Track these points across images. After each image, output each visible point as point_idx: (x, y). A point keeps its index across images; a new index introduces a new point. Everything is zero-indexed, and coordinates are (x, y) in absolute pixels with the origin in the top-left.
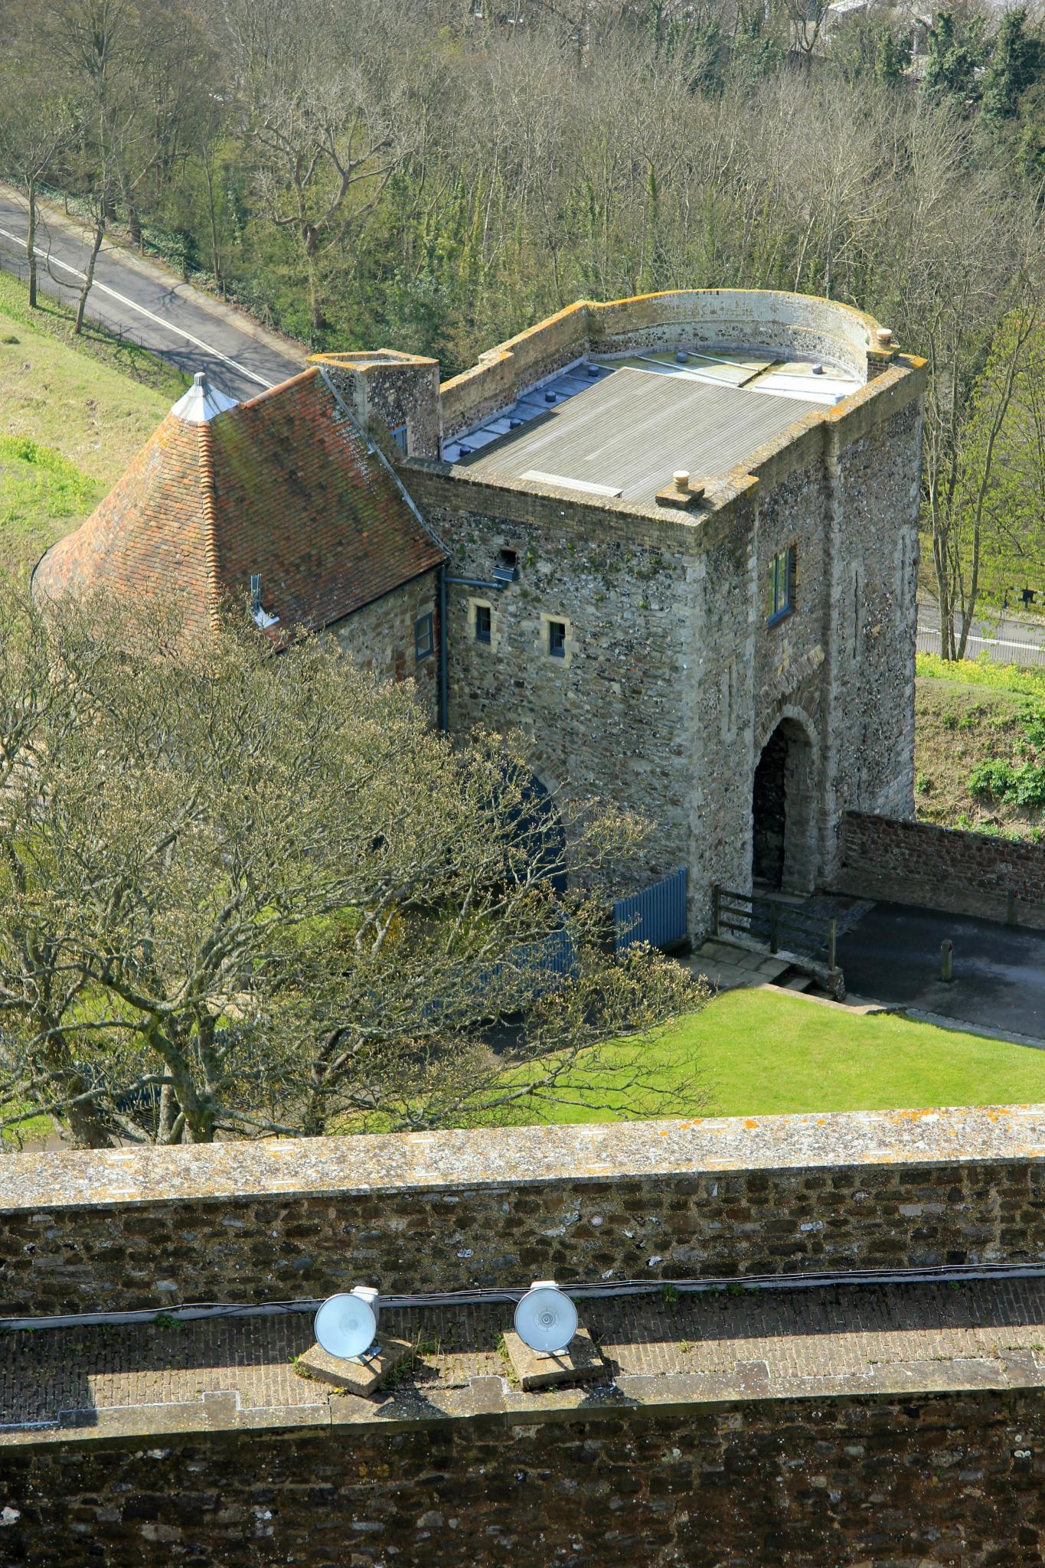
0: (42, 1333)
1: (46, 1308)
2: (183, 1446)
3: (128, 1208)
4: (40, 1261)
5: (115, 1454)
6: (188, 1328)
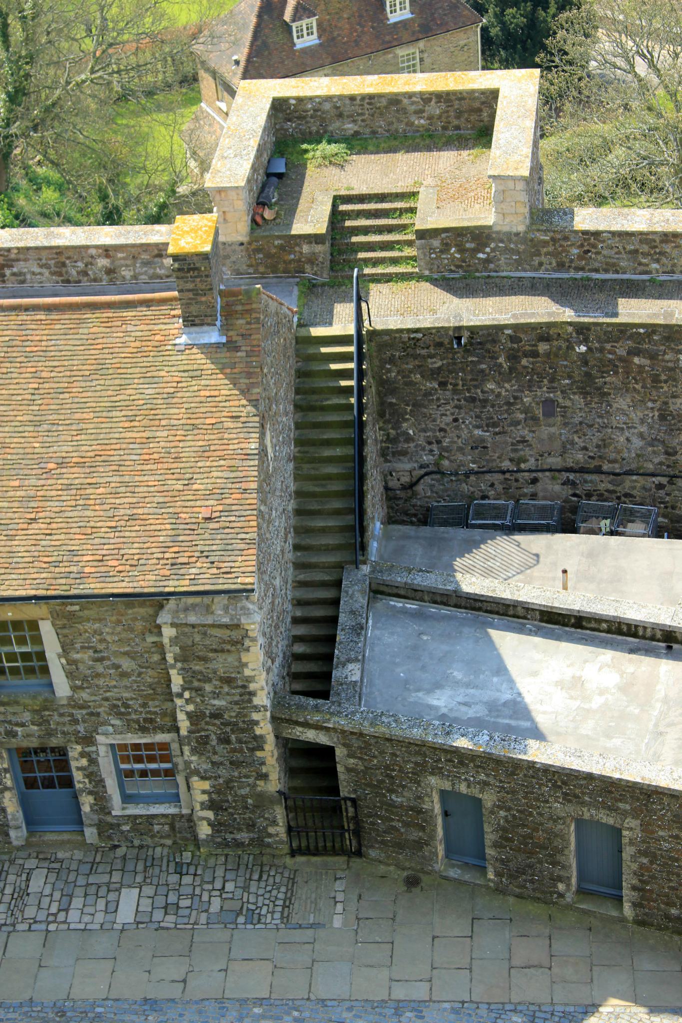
0: (604, 281)
1: (606, 271)
2: (652, 329)
3: (641, 233)
4: (605, 252)
5: (624, 329)
6: (662, 284)
